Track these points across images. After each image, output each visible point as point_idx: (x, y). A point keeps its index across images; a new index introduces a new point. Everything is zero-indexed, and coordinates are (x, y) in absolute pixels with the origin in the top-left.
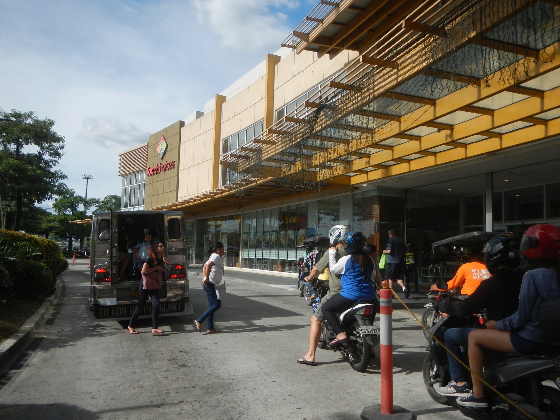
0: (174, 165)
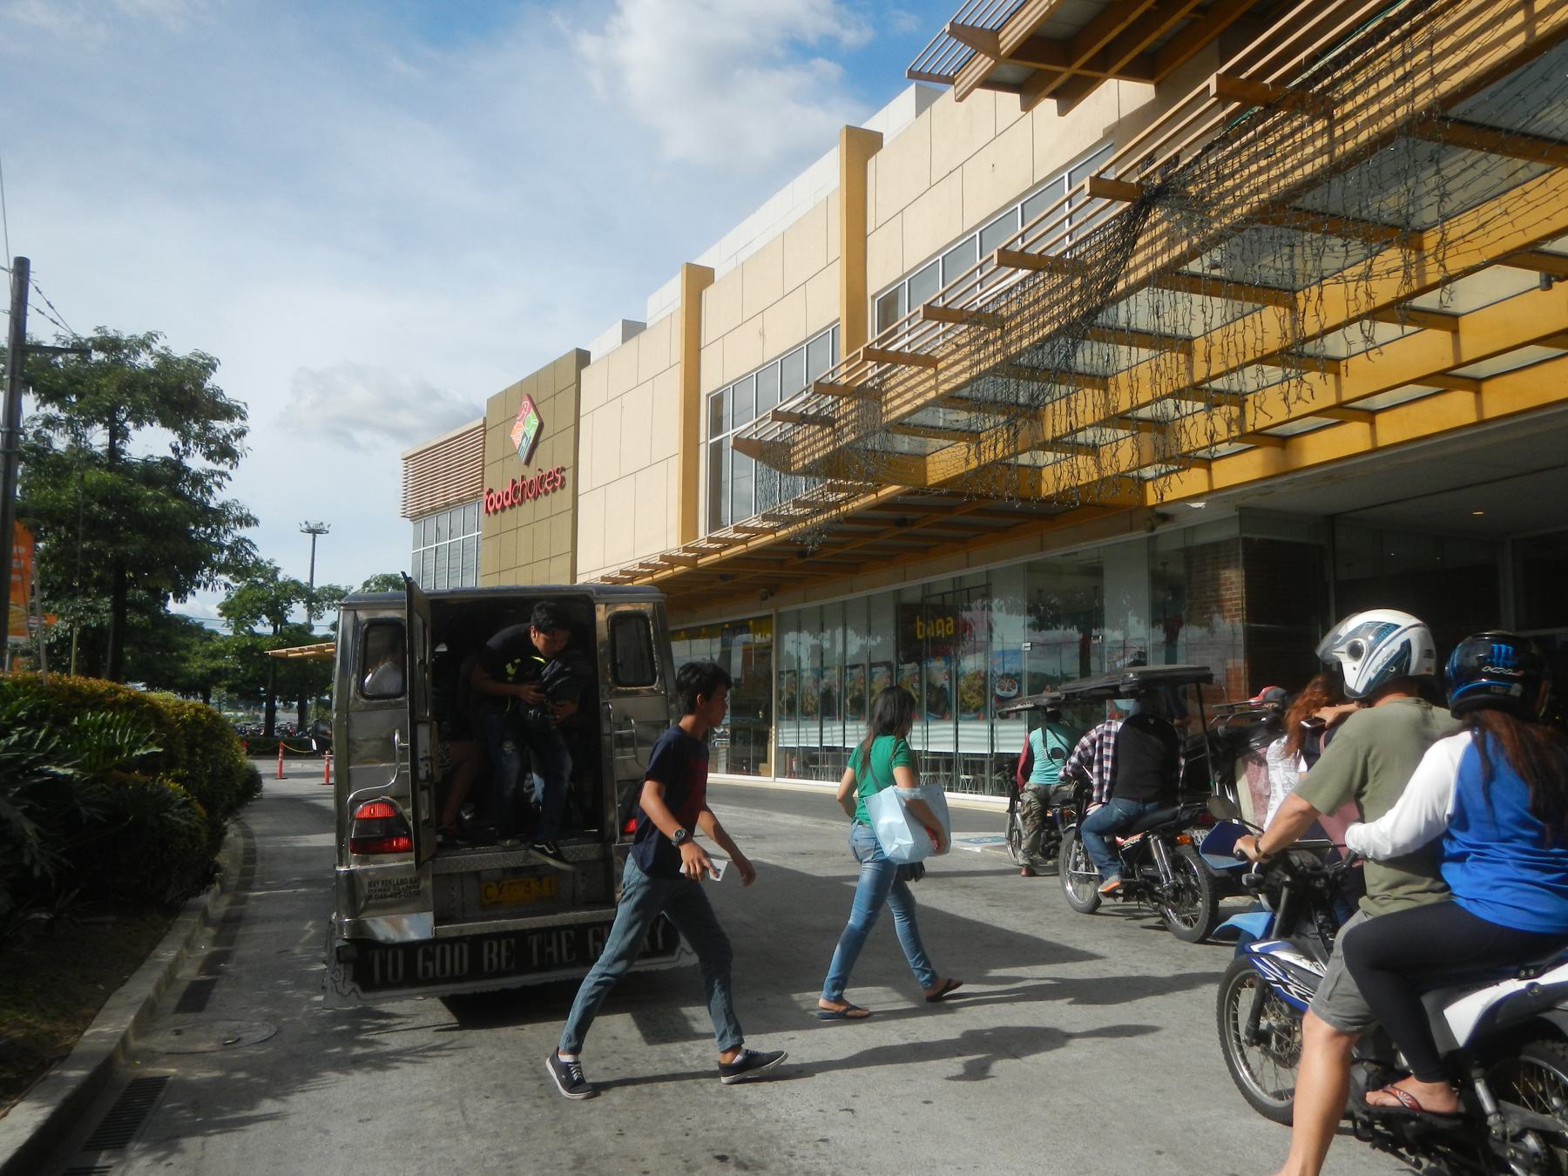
0: (563, 479)
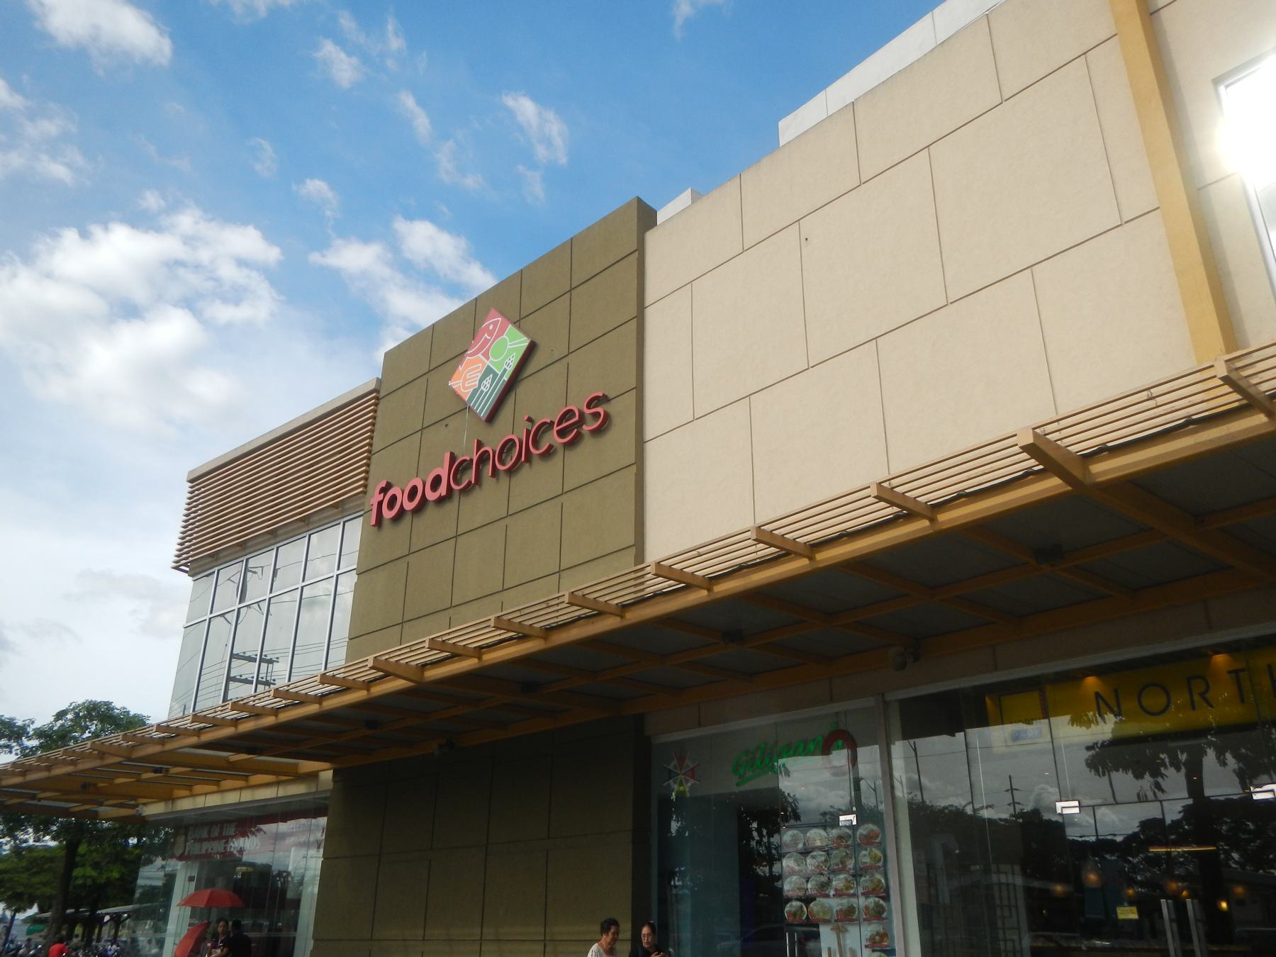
0: (607, 416)
